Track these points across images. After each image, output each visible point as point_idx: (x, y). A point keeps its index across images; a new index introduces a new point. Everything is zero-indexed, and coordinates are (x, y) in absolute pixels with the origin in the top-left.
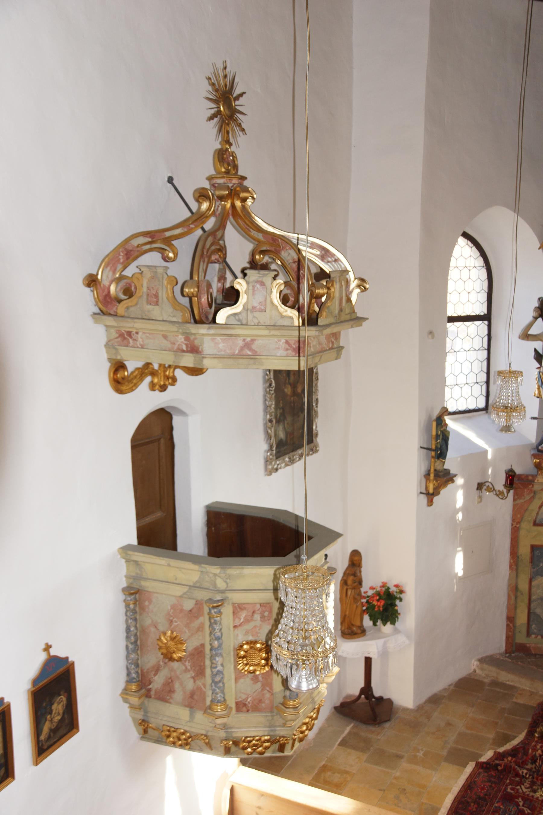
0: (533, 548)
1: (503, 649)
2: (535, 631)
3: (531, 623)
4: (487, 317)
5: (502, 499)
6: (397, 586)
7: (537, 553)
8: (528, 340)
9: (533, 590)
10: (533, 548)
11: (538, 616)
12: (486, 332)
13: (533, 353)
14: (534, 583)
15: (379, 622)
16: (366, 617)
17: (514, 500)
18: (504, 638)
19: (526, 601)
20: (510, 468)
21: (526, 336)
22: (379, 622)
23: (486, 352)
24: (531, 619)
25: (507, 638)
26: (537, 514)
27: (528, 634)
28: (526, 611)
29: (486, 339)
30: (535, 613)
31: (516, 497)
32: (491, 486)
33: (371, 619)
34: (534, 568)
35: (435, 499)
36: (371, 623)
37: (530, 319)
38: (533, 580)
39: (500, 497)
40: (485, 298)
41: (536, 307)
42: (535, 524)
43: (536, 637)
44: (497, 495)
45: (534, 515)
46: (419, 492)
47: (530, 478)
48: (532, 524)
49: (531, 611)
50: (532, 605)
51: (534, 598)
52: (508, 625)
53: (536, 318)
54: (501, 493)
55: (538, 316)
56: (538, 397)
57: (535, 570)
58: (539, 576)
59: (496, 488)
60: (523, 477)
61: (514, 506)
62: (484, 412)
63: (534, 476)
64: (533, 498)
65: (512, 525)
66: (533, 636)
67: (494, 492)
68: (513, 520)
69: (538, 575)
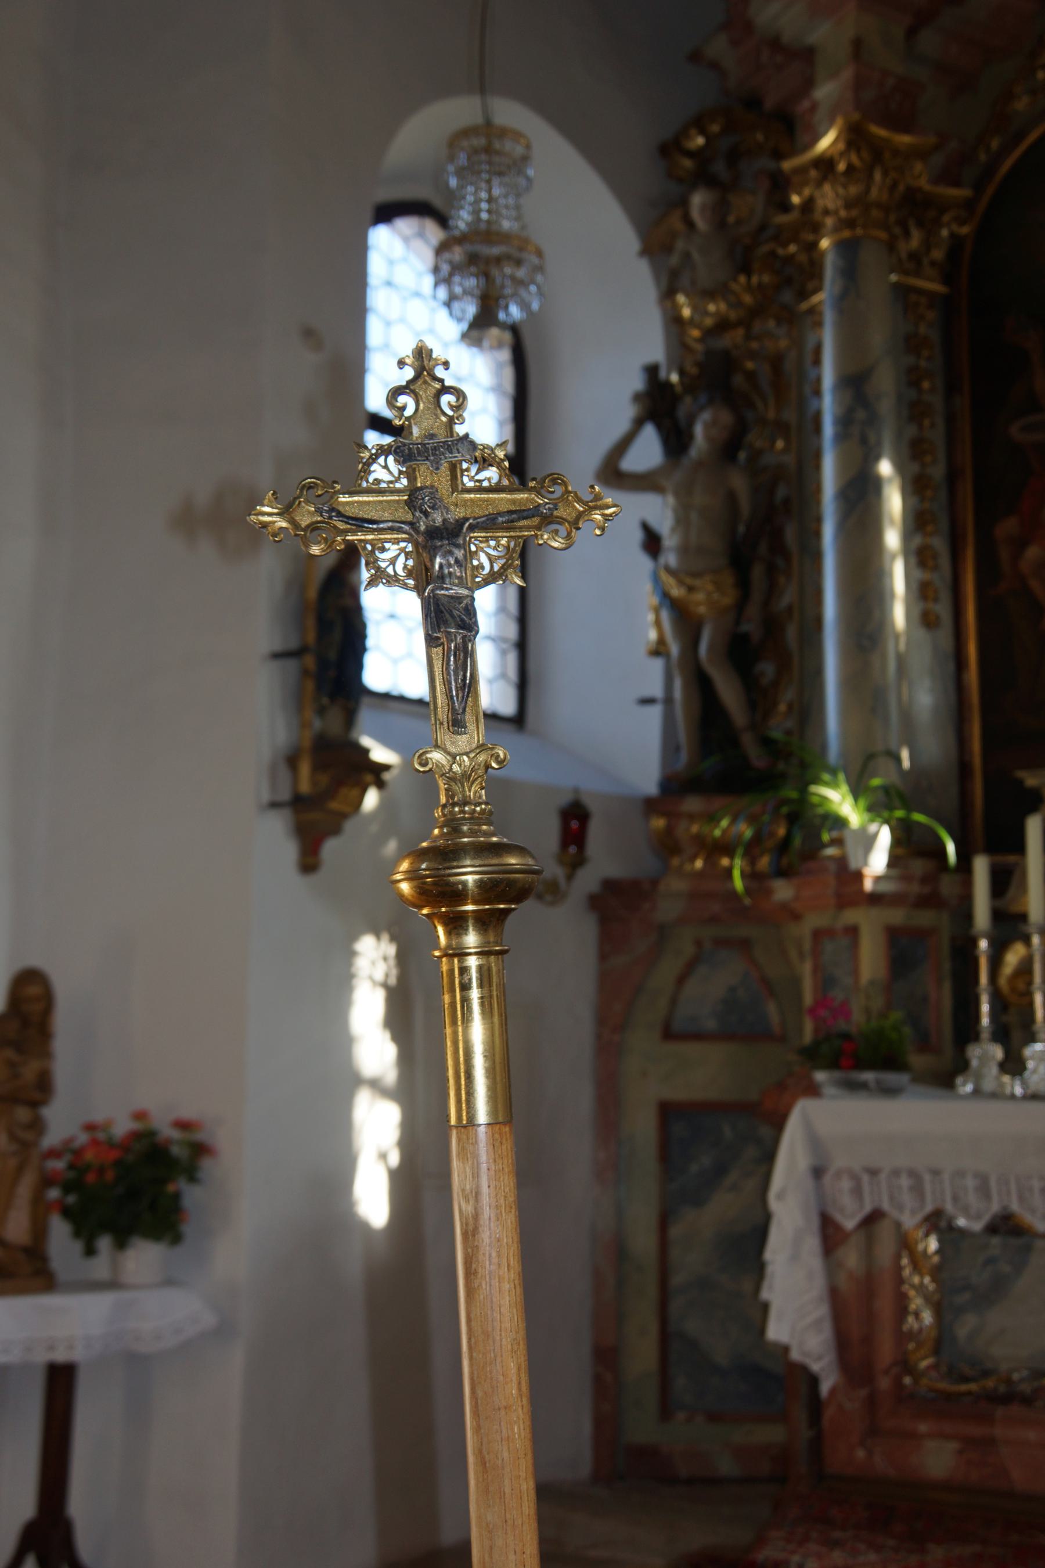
0: (668, 1112)
1: (585, 1469)
6: (183, 1125)
10: (668, 1112)
13: (638, 535)
14: (675, 1231)
15: (104, 1243)
16: (59, 1230)
17: (603, 957)
18: (587, 1427)
22: (104, 1243)
25: (600, 1422)
26: (674, 1001)
27: (666, 1411)
28: (654, 1328)
33: (77, 1234)
35: (330, 848)
36: (78, 1246)
42: (669, 1034)
46: (266, 797)
51: (677, 1280)
52: (598, 1380)
53: (638, 424)
63: (655, 883)
66: (681, 1416)
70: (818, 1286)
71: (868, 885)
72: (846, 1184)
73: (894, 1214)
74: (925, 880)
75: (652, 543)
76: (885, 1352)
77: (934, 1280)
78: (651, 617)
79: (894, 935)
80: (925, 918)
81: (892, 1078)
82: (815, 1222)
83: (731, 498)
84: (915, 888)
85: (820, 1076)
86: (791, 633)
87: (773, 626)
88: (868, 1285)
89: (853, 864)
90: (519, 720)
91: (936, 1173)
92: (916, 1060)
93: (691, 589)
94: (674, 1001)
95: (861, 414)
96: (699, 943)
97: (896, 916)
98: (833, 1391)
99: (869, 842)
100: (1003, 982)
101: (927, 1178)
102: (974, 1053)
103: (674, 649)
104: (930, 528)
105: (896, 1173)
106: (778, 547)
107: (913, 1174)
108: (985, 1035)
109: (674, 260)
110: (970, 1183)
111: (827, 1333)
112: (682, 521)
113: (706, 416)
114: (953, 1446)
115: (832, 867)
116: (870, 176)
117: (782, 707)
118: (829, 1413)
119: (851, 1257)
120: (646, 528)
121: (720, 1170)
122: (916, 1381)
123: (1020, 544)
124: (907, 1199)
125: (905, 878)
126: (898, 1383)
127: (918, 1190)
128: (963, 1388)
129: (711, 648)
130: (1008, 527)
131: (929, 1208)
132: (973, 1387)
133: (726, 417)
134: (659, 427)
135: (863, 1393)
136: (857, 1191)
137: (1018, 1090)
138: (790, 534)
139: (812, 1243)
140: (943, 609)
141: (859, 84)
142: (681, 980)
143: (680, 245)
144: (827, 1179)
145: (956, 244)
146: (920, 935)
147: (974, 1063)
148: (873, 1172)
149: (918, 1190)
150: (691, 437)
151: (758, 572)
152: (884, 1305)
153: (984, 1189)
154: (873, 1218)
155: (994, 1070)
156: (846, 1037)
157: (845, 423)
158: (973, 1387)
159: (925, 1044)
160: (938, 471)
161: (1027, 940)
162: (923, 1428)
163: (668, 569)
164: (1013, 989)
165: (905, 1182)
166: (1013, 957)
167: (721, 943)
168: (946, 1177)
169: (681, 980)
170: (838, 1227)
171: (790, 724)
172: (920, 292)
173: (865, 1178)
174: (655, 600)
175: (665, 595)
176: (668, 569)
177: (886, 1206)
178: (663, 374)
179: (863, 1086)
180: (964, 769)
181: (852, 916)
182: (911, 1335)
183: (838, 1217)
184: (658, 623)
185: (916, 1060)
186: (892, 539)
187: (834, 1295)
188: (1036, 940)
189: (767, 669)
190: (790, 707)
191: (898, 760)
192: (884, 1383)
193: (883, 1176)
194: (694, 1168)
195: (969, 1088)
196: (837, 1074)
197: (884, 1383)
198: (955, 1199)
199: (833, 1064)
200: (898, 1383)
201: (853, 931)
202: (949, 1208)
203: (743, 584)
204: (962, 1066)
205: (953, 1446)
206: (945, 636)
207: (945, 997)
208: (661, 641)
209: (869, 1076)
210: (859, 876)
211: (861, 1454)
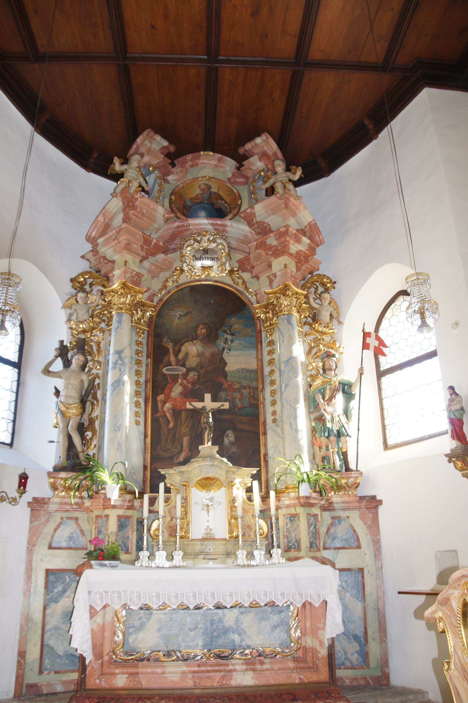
0: (48, 572)
2: (49, 666)
3: (44, 658)
4: (17, 365)
5: (14, 505)
7: (52, 578)
8: (49, 376)
9: (48, 619)
10: (48, 572)
11: (52, 648)
12: (16, 378)
13: (54, 390)
14: (48, 612)
17: (31, 522)
19: (40, 632)
20: (22, 471)
21: (47, 371)
23: (14, 395)
24: (45, 653)
26: (53, 536)
29: (15, 384)
30: (48, 645)
31: (33, 519)
32: (4, 495)
34: (48, 595)
37: (52, 357)
38: (47, 607)
39: (13, 503)
40: (17, 349)
41: (56, 348)
42: (50, 547)
43: (49, 674)
44: (10, 503)
45: (49, 537)
47: (47, 500)
48: (47, 547)
49: (45, 644)
50: (46, 636)
51: (47, 628)
53: (56, 357)
54: (14, 500)
55: (58, 355)
56: (56, 427)
57: (49, 596)
58: (53, 603)
59: (10, 496)
60: (40, 499)
61: (31, 528)
62: (9, 447)
64: (47, 521)
65: (28, 548)
67: (8, 501)
68: (29, 543)
69: (53, 602)
70: (88, 629)
71: (112, 503)
72: (98, 596)
73: (112, 605)
74: (129, 501)
75: (57, 393)
76: (107, 648)
77: (124, 625)
78: (55, 415)
79: (119, 517)
80: (130, 513)
81: (114, 563)
82: (88, 608)
83: (82, 381)
84: (127, 504)
85: (93, 562)
86: (97, 424)
87: (92, 421)
88: (103, 628)
89: (108, 497)
90: (11, 445)
91: (125, 592)
92: (123, 556)
93: (67, 408)
94: (53, 536)
95: (120, 362)
96: (62, 518)
97: (121, 512)
98: (90, 662)
99: (113, 490)
100: (152, 532)
101: (123, 593)
102: (141, 554)
103: (61, 426)
104: (139, 396)
105: (113, 592)
106: (95, 397)
107: (119, 593)
108: (145, 549)
109: (72, 311)
110: (135, 594)
111: (90, 644)
112: (66, 387)
113: (76, 357)
114: (126, 676)
115: (103, 497)
116: (127, 297)
117: (93, 446)
118: (88, 669)
119: (99, 619)
120: (56, 388)
121: (64, 591)
122: (116, 657)
123: (164, 403)
124: (116, 600)
125: (124, 501)
126: (111, 658)
127: (120, 598)
128: (130, 658)
129: (72, 427)
130: (161, 397)
131: (123, 603)
132: (133, 657)
133: (82, 358)
134: (62, 359)
135: (100, 662)
136: (101, 599)
137: (153, 565)
138: (99, 394)
139: (87, 615)
140: (142, 420)
141: (125, 272)
142: (55, 530)
143: (74, 307)
144: (92, 595)
145: (151, 317)
146: (128, 518)
147: (141, 557)
148: (106, 592)
149: (120, 598)
150: (71, 363)
151: (88, 404)
152: (107, 634)
153: (139, 597)
154: (105, 607)
155: (147, 559)
156: (102, 550)
157: (115, 364)
158: (133, 657)
159: (127, 552)
160: (142, 380)
161: (158, 519)
162: (117, 671)
163: (61, 402)
164: (154, 535)
165: (116, 595)
166: (155, 525)
167: (69, 518)
168: (128, 593)
169: (55, 530)
170: (95, 610)
171: (94, 451)
172: (141, 329)
173: (104, 594)
174: (56, 411)
175: (59, 409)
176: (61, 402)
177: (110, 603)
178: (65, 344)
179: (105, 565)
180: (145, 467)
181: (107, 512)
182: (116, 642)
183: (95, 607)
184: (57, 418)
185: (123, 556)
186: (127, 398)
187: (92, 630)
188: (161, 520)
189: (89, 434)
190: (95, 446)
191: (125, 465)
192: (106, 658)
193: (109, 593)
194: (56, 590)
195: (139, 565)
196: (97, 561)
197: (106, 658)
198: (130, 600)
199: (97, 558)
200: (111, 658)
201: (107, 516)
202: (129, 603)
203: (84, 408)
204: (138, 558)
205: (126, 676)
206: (142, 427)
207: (134, 537)
208: (57, 424)
209: (107, 562)
210: (110, 499)
211: (98, 681)
